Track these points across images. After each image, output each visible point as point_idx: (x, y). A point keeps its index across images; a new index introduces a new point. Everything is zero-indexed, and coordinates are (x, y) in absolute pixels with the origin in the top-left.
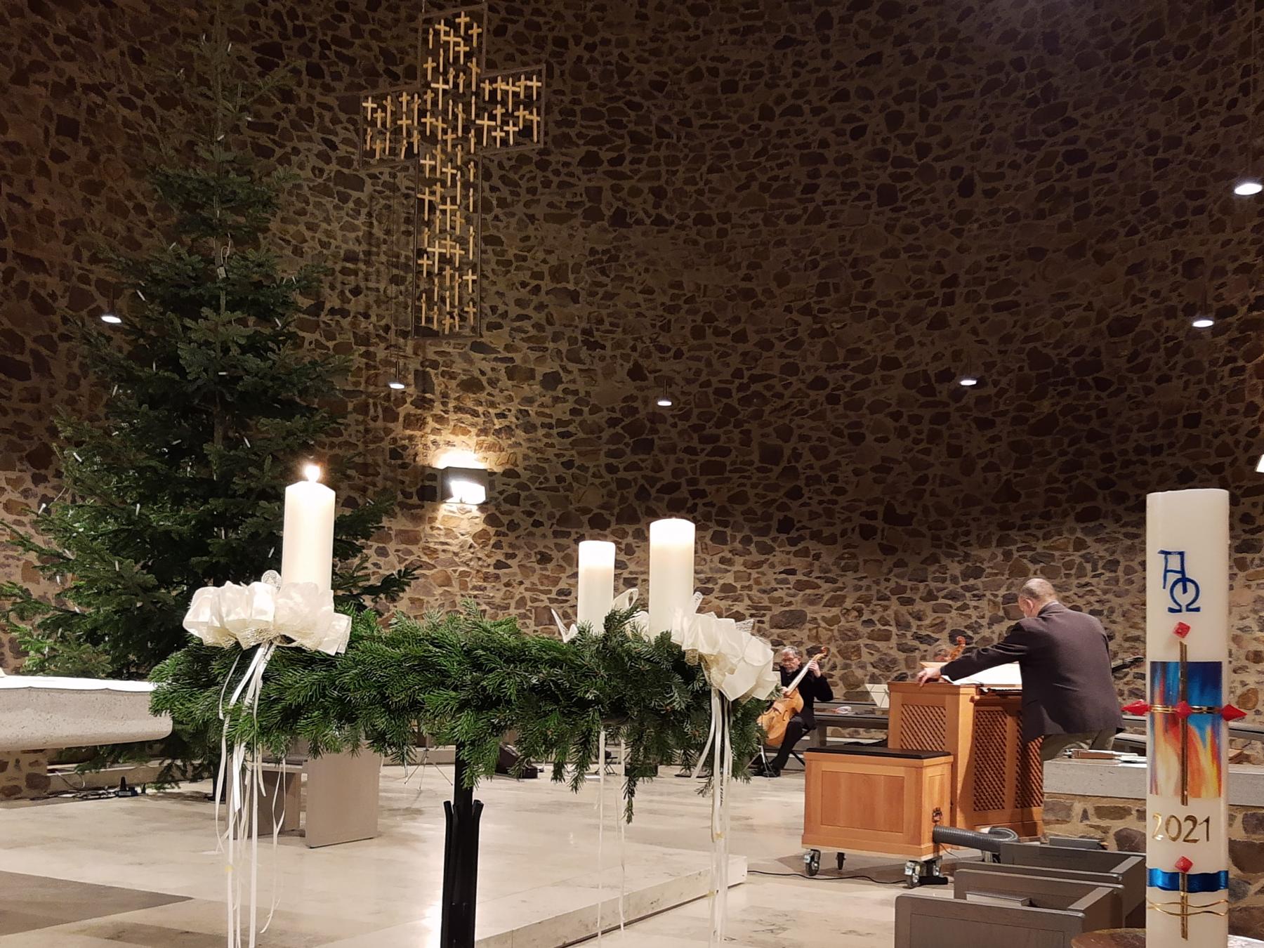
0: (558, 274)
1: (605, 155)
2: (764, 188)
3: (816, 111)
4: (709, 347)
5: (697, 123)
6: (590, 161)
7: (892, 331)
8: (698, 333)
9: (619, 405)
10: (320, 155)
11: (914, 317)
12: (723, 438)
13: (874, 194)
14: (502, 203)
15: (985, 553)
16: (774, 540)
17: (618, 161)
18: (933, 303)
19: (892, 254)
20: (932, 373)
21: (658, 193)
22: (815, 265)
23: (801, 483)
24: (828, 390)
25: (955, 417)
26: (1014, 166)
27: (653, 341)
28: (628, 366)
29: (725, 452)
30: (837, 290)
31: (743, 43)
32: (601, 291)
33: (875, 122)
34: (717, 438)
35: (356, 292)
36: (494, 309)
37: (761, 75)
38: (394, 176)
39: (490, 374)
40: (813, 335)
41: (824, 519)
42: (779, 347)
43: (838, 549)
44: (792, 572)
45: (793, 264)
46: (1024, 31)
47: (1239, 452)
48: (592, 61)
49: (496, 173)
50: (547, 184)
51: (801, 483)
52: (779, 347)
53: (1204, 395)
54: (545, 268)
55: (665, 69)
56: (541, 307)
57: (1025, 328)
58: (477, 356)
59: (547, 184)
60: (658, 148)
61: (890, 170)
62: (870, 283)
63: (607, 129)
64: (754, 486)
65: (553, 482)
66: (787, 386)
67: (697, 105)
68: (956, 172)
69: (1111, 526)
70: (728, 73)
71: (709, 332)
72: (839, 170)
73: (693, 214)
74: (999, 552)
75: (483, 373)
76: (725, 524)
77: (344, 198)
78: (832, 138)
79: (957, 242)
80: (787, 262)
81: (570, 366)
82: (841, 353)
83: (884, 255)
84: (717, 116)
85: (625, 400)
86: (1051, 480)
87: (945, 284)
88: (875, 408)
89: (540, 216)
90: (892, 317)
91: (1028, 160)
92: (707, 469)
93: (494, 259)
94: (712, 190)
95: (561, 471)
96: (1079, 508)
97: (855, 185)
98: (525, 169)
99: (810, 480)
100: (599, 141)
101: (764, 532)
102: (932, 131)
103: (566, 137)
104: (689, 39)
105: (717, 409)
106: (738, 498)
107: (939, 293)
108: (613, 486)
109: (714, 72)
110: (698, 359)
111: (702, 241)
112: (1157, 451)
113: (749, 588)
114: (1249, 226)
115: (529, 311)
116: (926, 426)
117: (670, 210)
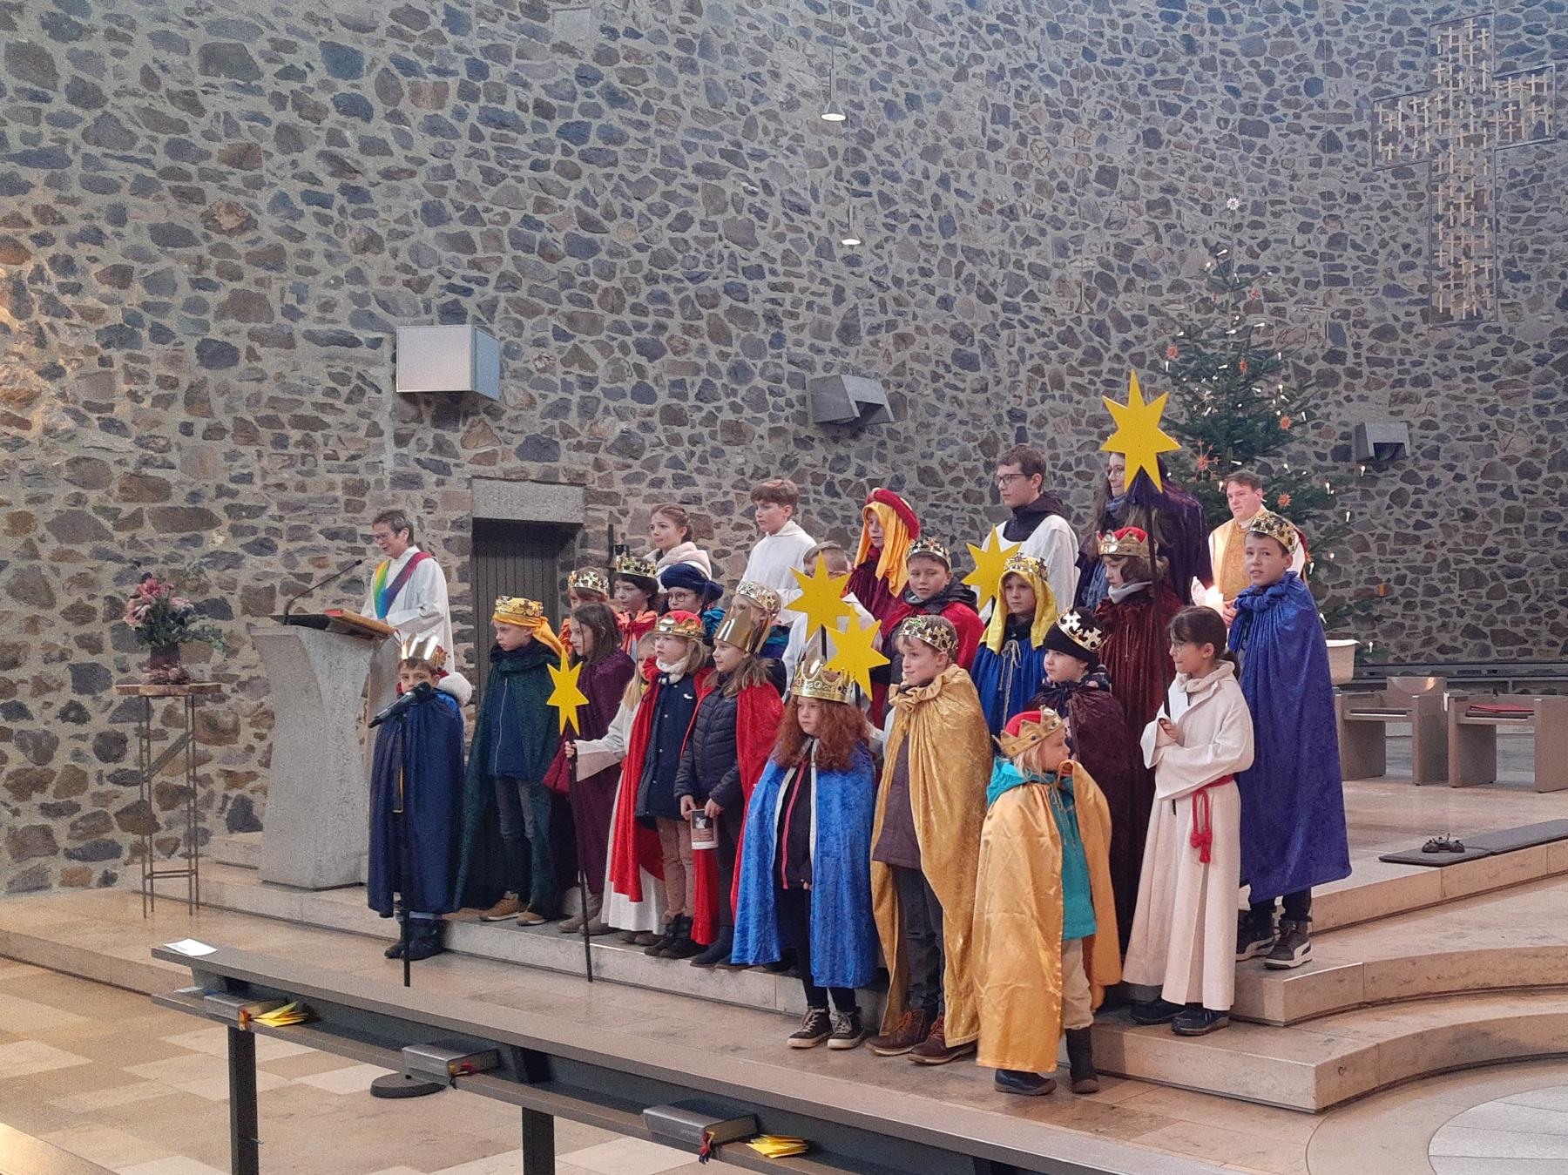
10: (1224, 105)
35: (1265, 245)
36: (1406, 247)
38: (1297, 116)
39: (1404, 319)
58: (1389, 301)
65: (1475, 432)
75: (1396, 318)
93: (1404, 193)
95: (1485, 417)
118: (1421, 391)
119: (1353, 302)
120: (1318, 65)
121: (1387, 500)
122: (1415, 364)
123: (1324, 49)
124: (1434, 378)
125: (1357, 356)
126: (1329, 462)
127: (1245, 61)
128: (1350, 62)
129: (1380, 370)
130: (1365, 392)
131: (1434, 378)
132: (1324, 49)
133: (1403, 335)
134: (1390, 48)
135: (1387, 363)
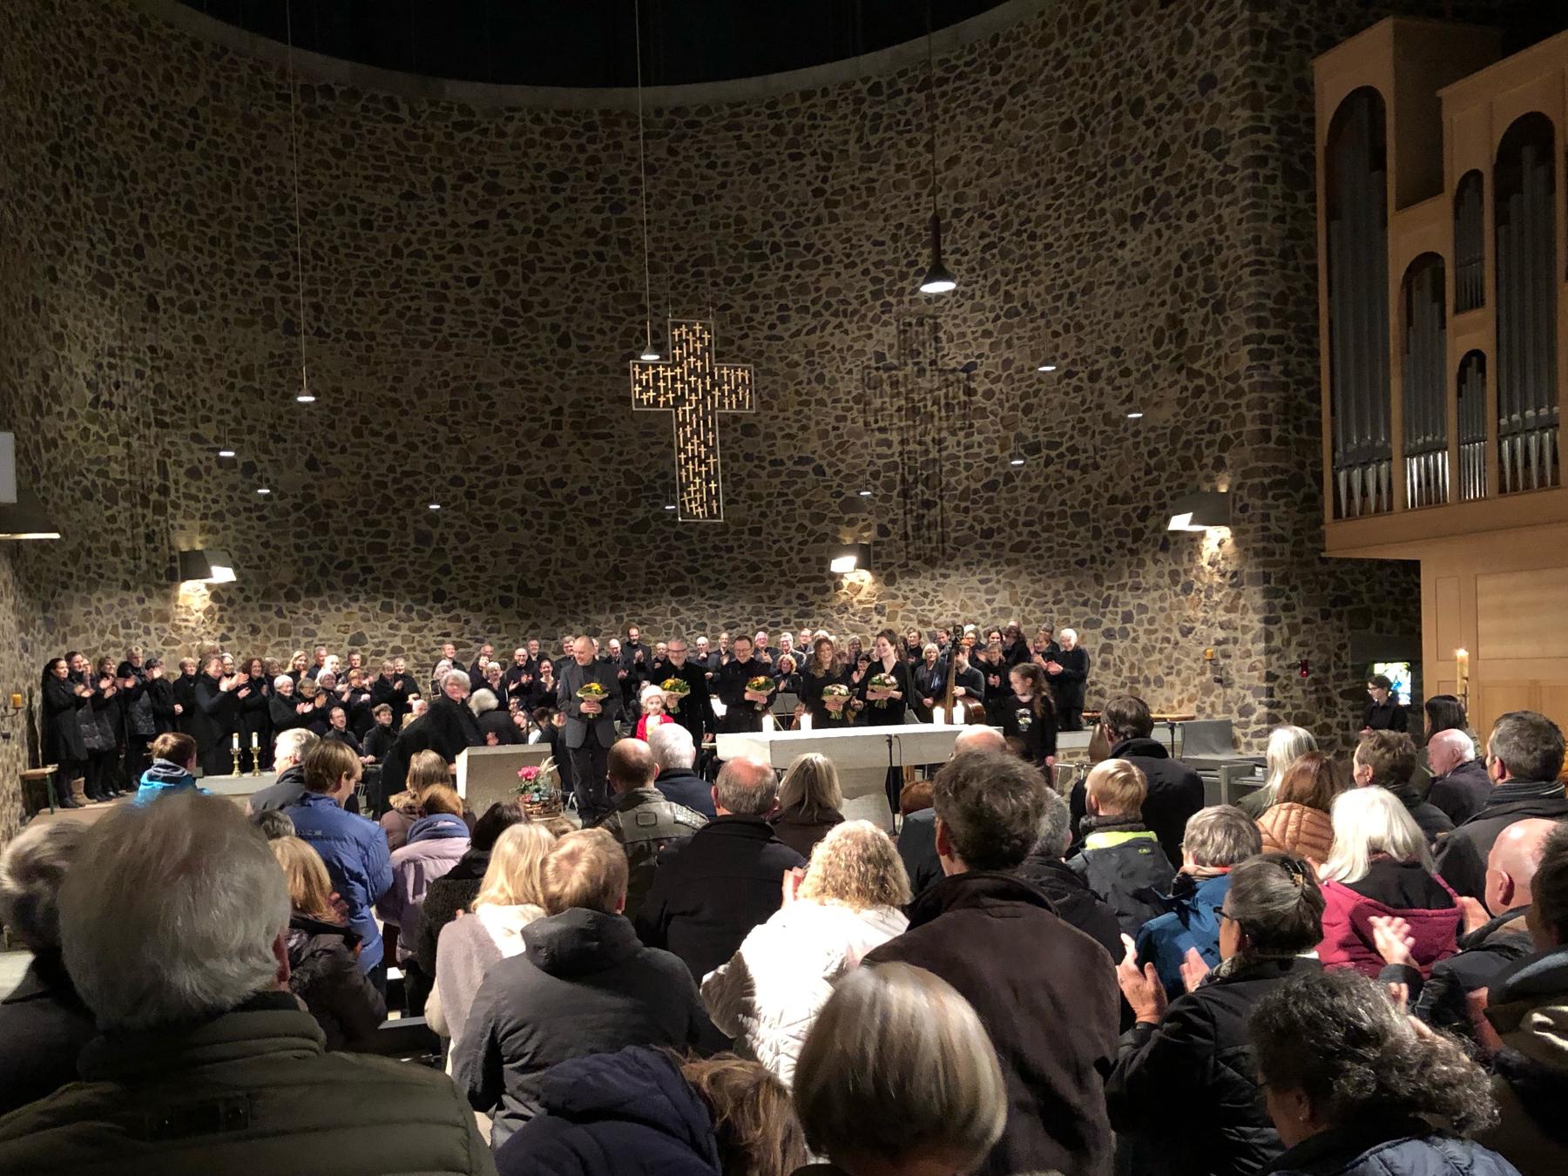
0: (247, 373)
1: (275, 270)
2: (401, 315)
3: (437, 258)
4: (367, 445)
5: (343, 251)
6: (264, 273)
7: (513, 445)
8: (358, 433)
9: (300, 492)
11: (530, 435)
12: (384, 523)
13: (489, 333)
14: (204, 306)
15: (601, 618)
16: (431, 608)
17: (284, 276)
18: (545, 426)
19: (508, 383)
20: (548, 478)
21: (317, 308)
22: (446, 384)
23: (450, 562)
24: (465, 488)
25: (570, 517)
26: (601, 331)
27: (324, 437)
28: (305, 458)
29: (386, 534)
30: (466, 406)
31: (374, 189)
32: (280, 391)
33: (487, 277)
34: (379, 523)
36: (203, 402)
37: (390, 219)
38: (130, 275)
39: (205, 463)
40: (449, 442)
41: (470, 591)
42: (423, 449)
43: (483, 616)
44: (447, 635)
45: (428, 381)
46: (603, 233)
47: (793, 555)
48: (259, 183)
49: (197, 278)
50: (234, 291)
51: (450, 562)
52: (423, 449)
53: (763, 515)
54: (237, 368)
55: (316, 200)
56: (236, 402)
57: (620, 454)
58: (195, 446)
59: (234, 291)
60: (314, 269)
61: (502, 316)
62: (492, 405)
63: (275, 247)
64: (412, 563)
66: (431, 482)
67: (342, 236)
68: (555, 328)
69: (697, 600)
70: (365, 212)
71: (366, 432)
72: (459, 309)
73: (345, 330)
74: (612, 617)
76: (391, 596)
77: (104, 297)
78: (452, 282)
79: (560, 382)
80: (424, 379)
81: (264, 457)
82: (473, 458)
83: (503, 384)
84: (358, 248)
85: (305, 487)
86: (649, 566)
87: (553, 413)
88: (505, 504)
89: (231, 320)
90: (512, 434)
91: (613, 329)
92: (372, 548)
94: (359, 311)
96: (673, 586)
97: (474, 324)
98: (218, 275)
99: (458, 559)
100: (268, 256)
101: (423, 601)
102: (534, 292)
103: (244, 248)
104: (332, 177)
105: (377, 497)
106: (400, 574)
107: (549, 419)
108: (300, 563)
109: (354, 210)
110: (359, 455)
111: (354, 354)
112: (730, 549)
113: (414, 649)
114: (791, 410)
115: (229, 406)
116: (546, 519)
117: (327, 324)
118: (220, 525)
119: (172, 443)
120: (141, 232)
121: (200, 614)
122: (215, 501)
123: (144, 219)
124: (228, 516)
125: (177, 491)
126: (163, 581)
127: (97, 217)
128: (162, 236)
129: (192, 503)
130: (182, 522)
131: (228, 516)
132: (144, 219)
133: (205, 477)
134: (185, 232)
135: (197, 499)
